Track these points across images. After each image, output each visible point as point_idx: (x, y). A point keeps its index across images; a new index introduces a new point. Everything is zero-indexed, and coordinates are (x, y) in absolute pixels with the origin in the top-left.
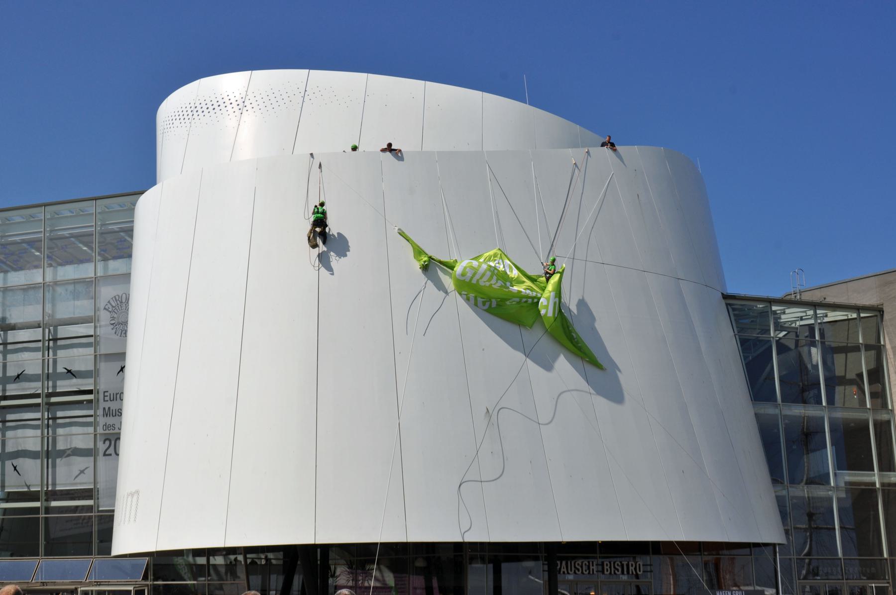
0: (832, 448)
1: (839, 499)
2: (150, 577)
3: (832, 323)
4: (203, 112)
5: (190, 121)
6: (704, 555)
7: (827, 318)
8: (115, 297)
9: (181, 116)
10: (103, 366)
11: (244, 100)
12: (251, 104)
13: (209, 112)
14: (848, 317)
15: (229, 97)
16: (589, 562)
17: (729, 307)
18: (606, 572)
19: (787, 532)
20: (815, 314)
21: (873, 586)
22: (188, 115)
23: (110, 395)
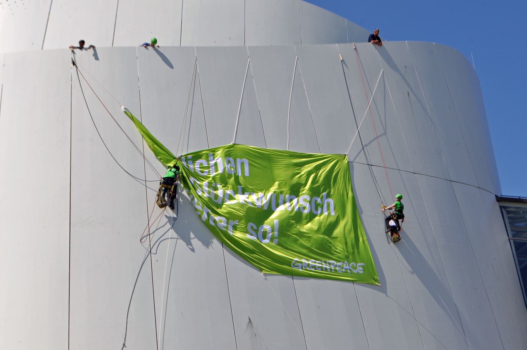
17: (503, 210)
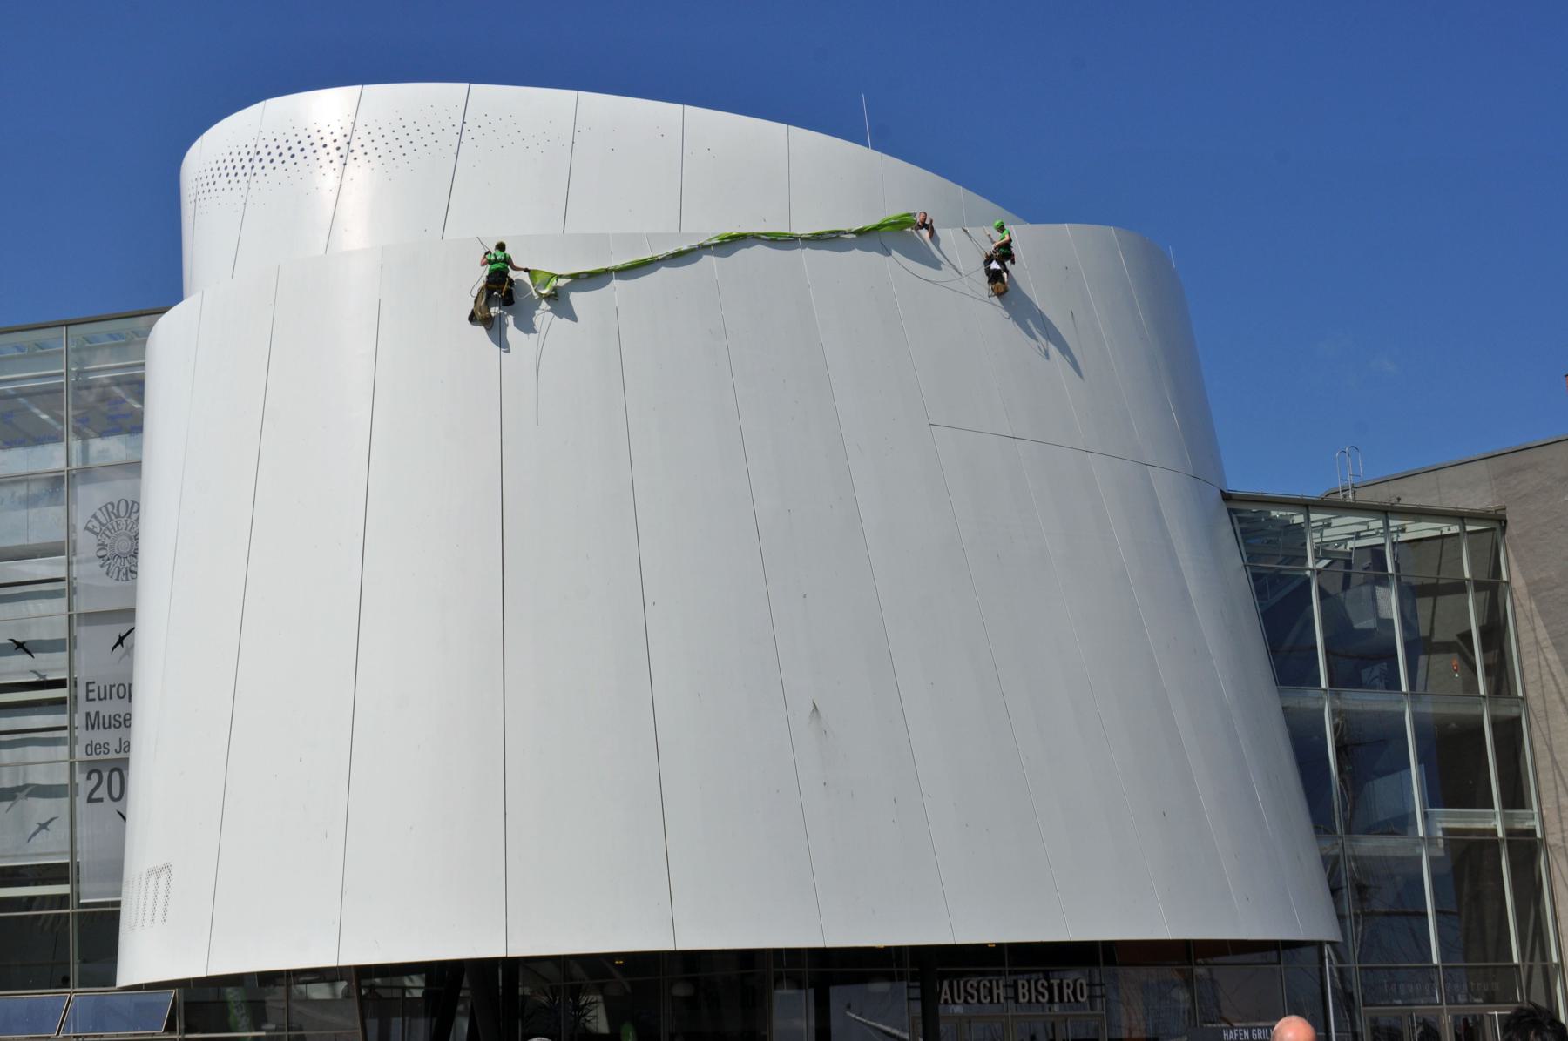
0: (1420, 768)
1: (1433, 861)
2: (180, 1024)
3: (1413, 544)
4: (272, 161)
5: (247, 178)
6: (1197, 964)
8: (106, 506)
9: (230, 170)
10: (82, 632)
11: (348, 140)
12: (362, 146)
13: (283, 162)
14: (1441, 531)
15: (321, 135)
16: (991, 982)
17: (1234, 516)
18: (1021, 1000)
19: (1341, 918)
20: (1387, 526)
21: (1494, 1015)
23: (99, 687)
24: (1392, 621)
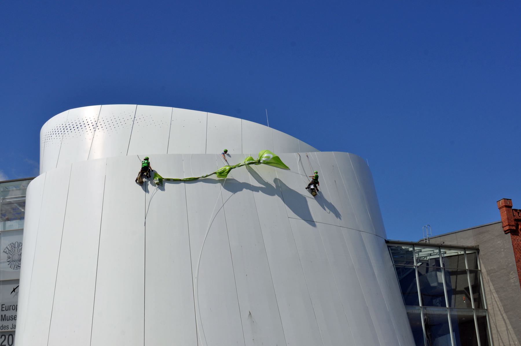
0: (453, 334)
5: (62, 135)
7: (446, 254)
8: (11, 244)
9: (57, 132)
12: (101, 125)
13: (75, 130)
15: (87, 121)
17: (389, 248)
20: (440, 252)
22: (61, 131)
23: (6, 306)
24: (442, 283)
